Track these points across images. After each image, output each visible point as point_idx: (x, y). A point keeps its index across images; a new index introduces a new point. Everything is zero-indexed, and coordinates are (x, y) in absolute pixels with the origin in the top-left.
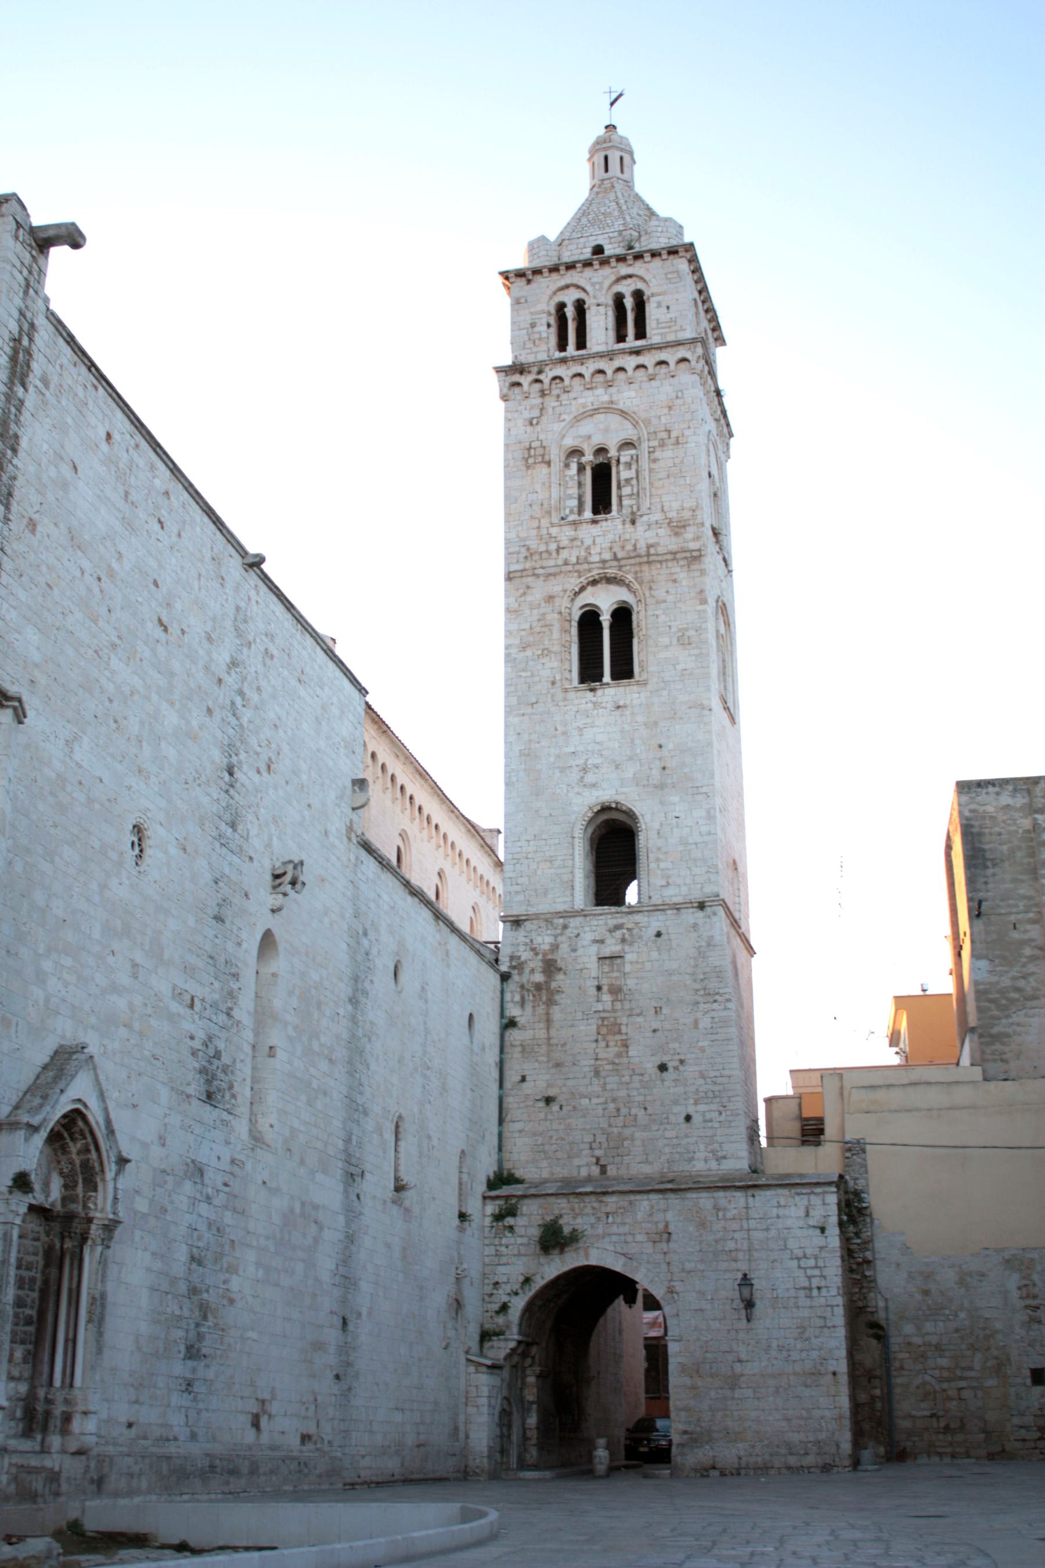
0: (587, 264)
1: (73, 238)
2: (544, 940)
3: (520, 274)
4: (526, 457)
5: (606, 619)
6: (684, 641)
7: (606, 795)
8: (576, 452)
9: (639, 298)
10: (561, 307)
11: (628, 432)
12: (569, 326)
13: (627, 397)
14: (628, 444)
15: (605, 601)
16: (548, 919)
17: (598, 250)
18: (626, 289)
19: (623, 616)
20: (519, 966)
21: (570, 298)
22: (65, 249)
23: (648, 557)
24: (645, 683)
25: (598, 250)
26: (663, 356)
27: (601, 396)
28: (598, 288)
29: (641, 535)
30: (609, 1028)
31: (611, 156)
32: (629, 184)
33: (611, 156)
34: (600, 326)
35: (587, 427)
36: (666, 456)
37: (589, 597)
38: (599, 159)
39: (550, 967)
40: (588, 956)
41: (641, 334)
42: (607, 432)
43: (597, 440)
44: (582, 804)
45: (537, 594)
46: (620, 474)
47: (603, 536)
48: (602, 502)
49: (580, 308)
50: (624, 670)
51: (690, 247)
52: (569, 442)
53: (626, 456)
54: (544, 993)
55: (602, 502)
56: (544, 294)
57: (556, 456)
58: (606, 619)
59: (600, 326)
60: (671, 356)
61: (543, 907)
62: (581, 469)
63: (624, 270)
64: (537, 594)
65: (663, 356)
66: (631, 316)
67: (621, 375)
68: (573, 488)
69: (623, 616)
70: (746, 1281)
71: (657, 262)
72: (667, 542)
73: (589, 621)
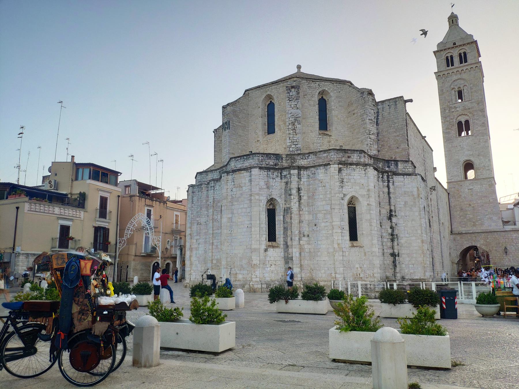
0: (452, 48)
1: (411, 101)
3: (437, 51)
5: (463, 123)
9: (465, 54)
10: (447, 58)
12: (449, 62)
17: (455, 44)
21: (449, 55)
22: (410, 103)
26: (472, 66)
27: (459, 76)
28: (455, 54)
31: (453, 20)
32: (458, 25)
33: (453, 20)
34: (456, 60)
35: (456, 83)
38: (451, 20)
42: (460, 84)
49: (452, 57)
51: (476, 41)
52: (452, 87)
56: (444, 55)
58: (463, 123)
59: (456, 60)
60: (474, 66)
62: (455, 91)
63: (461, 48)
65: (472, 66)
66: (463, 58)
67: (463, 71)
69: (467, 122)
70: (506, 248)
71: (468, 46)
73: (460, 124)
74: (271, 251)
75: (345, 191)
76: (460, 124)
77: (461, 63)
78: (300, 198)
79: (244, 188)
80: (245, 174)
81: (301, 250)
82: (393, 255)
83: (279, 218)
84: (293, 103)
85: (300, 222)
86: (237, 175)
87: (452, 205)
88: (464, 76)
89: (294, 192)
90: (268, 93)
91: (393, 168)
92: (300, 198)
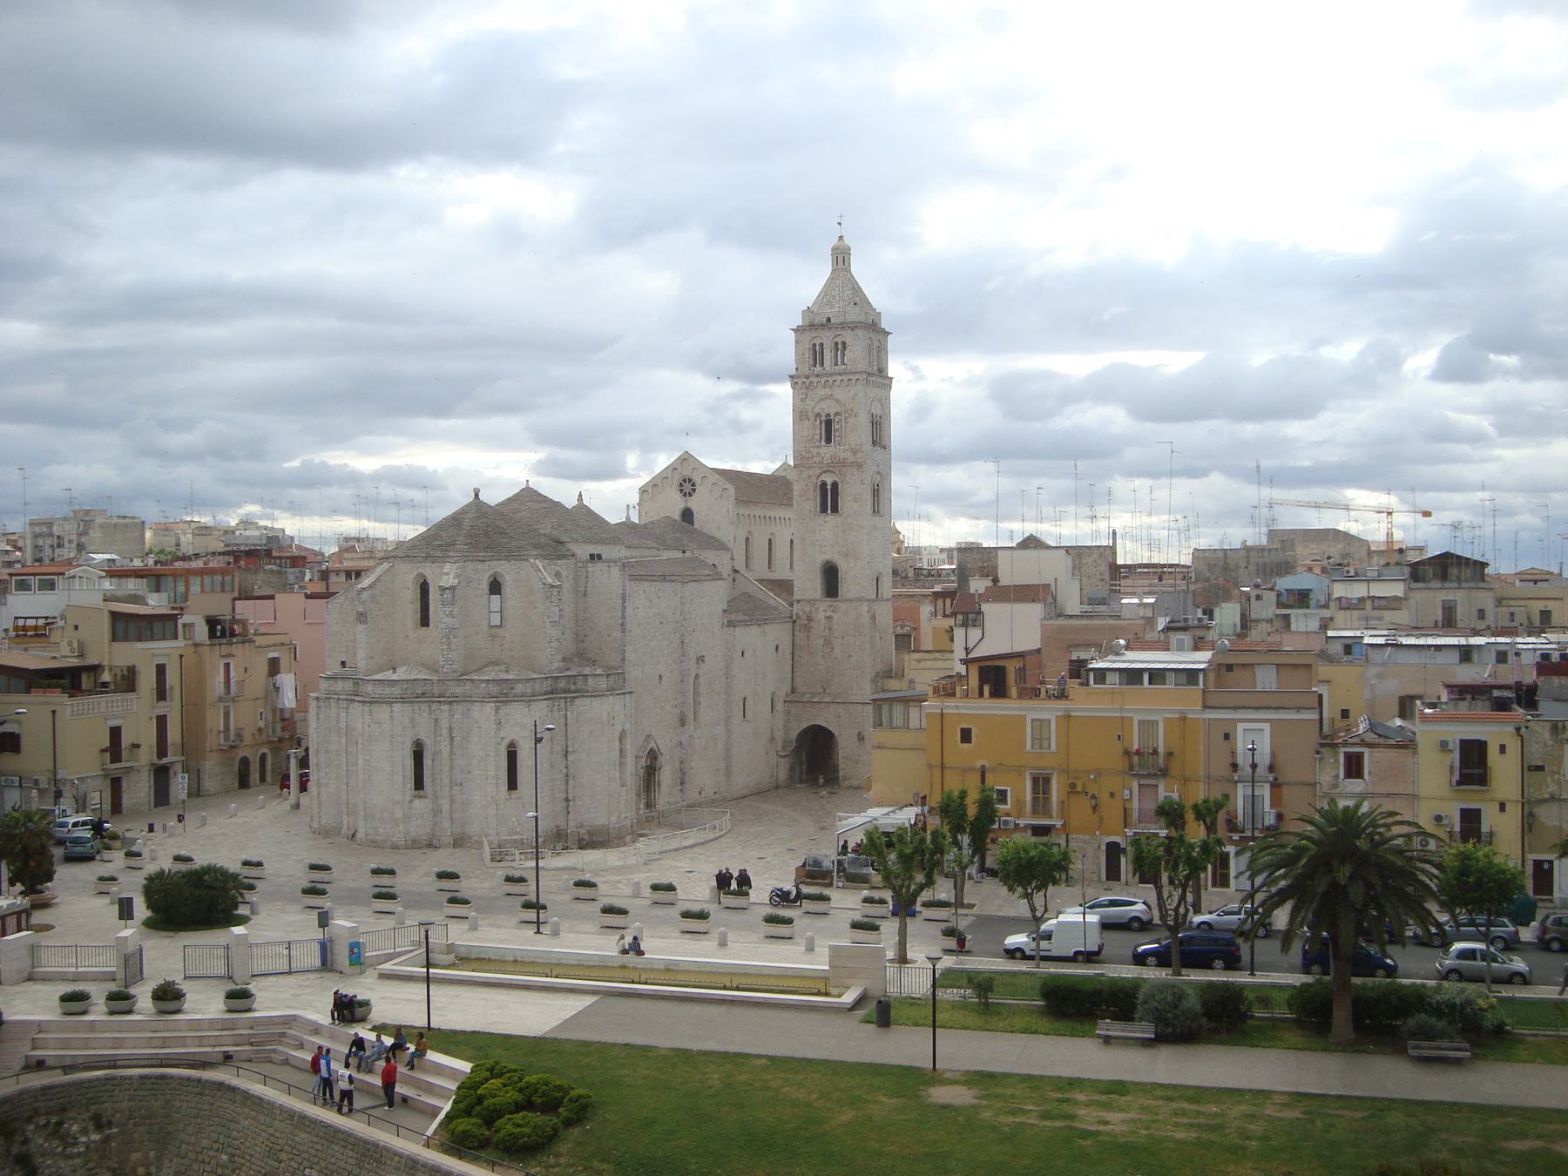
2: (807, 609)
4: (800, 415)
6: (855, 500)
7: (828, 557)
8: (818, 415)
11: (838, 409)
12: (817, 355)
13: (839, 393)
14: (837, 414)
15: (829, 479)
16: (809, 601)
17: (829, 320)
18: (839, 340)
19: (835, 485)
20: (799, 617)
23: (843, 464)
25: (829, 320)
27: (828, 391)
29: (842, 455)
30: (828, 642)
33: (841, 256)
35: (823, 405)
36: (851, 420)
37: (823, 478)
39: (809, 619)
40: (822, 616)
42: (829, 408)
44: (820, 559)
45: (804, 475)
46: (835, 426)
47: (827, 452)
48: (828, 440)
50: (835, 509)
54: (807, 628)
55: (828, 440)
57: (811, 416)
59: (828, 356)
61: (807, 597)
64: (804, 475)
68: (818, 431)
69: (835, 485)
72: (851, 458)
74: (417, 802)
75: (502, 734)
76: (824, 485)
78: (452, 739)
80: (386, 708)
81: (452, 801)
82: (567, 800)
83: (427, 762)
84: (447, 609)
85: (452, 768)
86: (375, 708)
87: (797, 642)
88: (839, 393)
89: (445, 732)
91: (580, 685)
92: (452, 739)
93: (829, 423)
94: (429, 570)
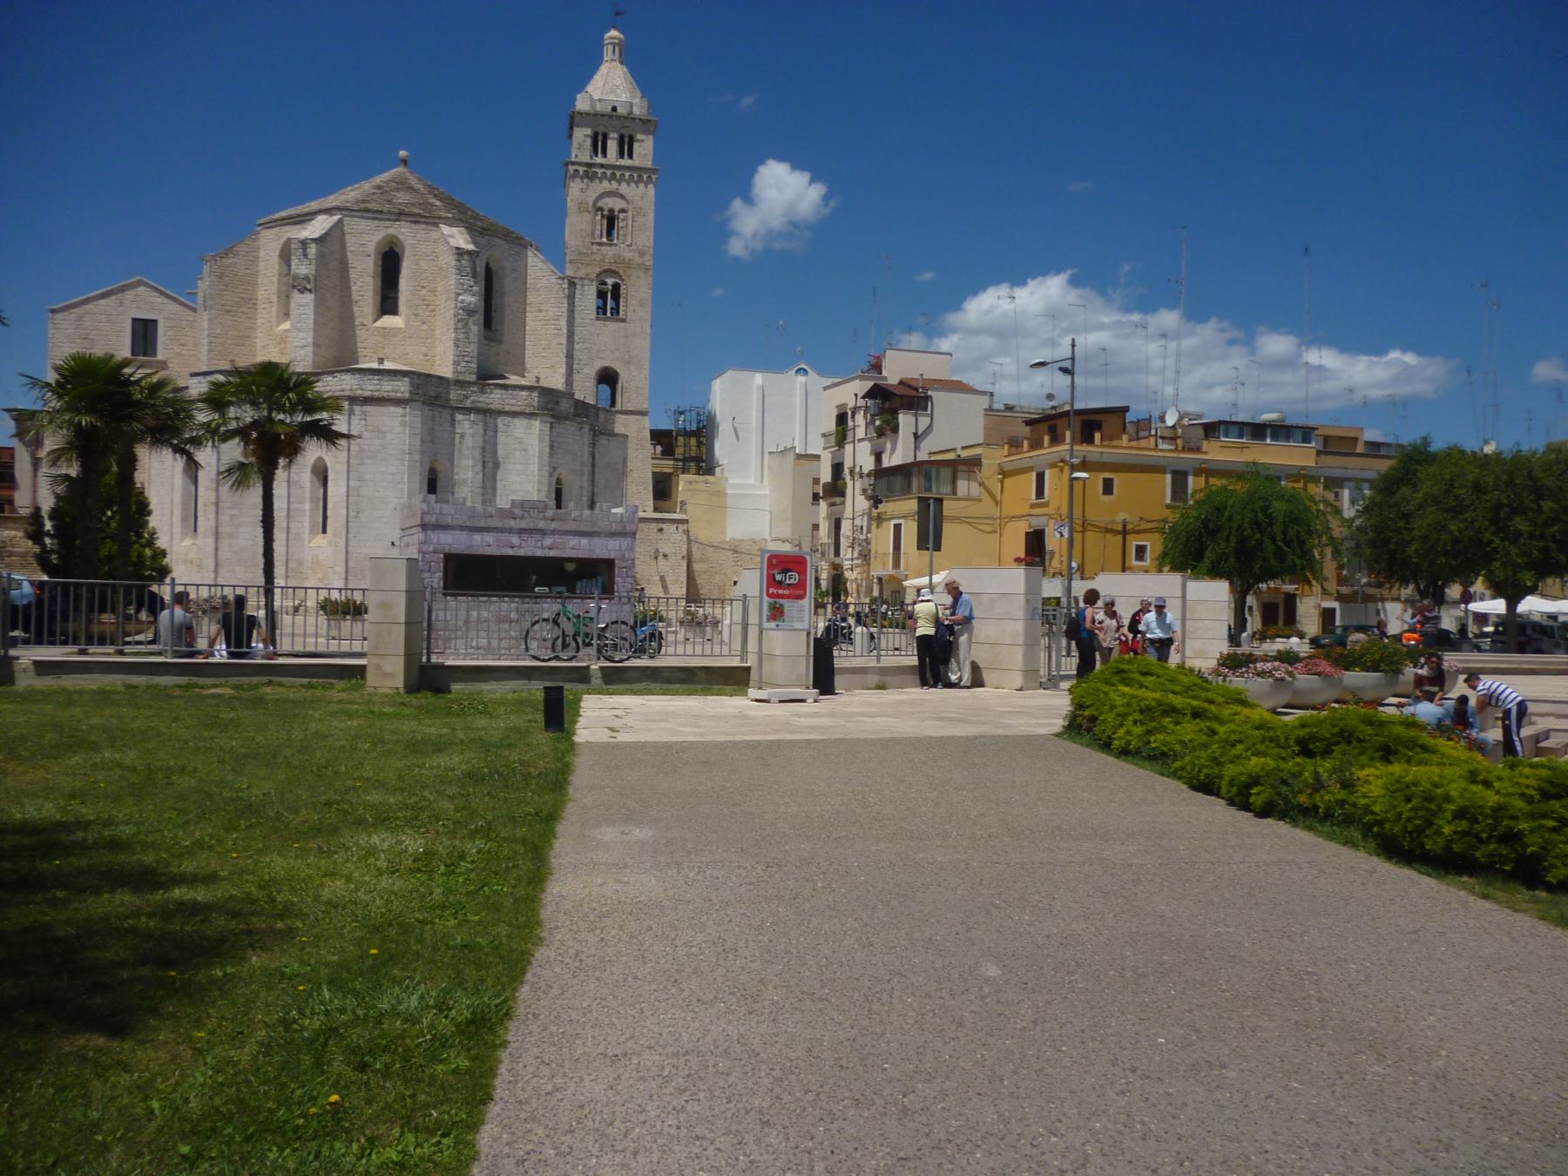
13: (624, 189)
14: (623, 211)
17: (614, 109)
18: (626, 132)
19: (616, 287)
21: (601, 130)
24: (624, 321)
25: (614, 109)
27: (614, 185)
29: (628, 255)
34: (612, 146)
41: (631, 156)
43: (610, 206)
50: (616, 310)
53: (622, 216)
59: (612, 146)
69: (616, 287)
77: (621, 155)
79: (389, 436)
90: (391, 231)
93: (611, 221)
94: (405, 232)
